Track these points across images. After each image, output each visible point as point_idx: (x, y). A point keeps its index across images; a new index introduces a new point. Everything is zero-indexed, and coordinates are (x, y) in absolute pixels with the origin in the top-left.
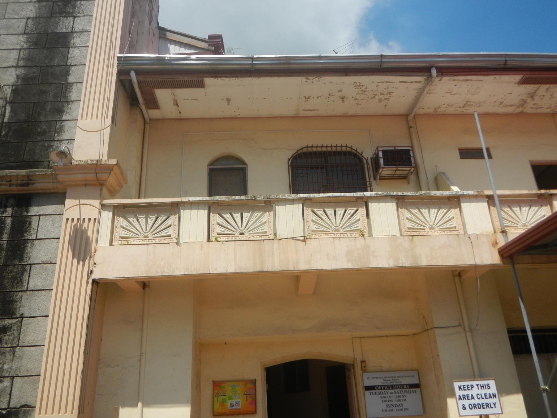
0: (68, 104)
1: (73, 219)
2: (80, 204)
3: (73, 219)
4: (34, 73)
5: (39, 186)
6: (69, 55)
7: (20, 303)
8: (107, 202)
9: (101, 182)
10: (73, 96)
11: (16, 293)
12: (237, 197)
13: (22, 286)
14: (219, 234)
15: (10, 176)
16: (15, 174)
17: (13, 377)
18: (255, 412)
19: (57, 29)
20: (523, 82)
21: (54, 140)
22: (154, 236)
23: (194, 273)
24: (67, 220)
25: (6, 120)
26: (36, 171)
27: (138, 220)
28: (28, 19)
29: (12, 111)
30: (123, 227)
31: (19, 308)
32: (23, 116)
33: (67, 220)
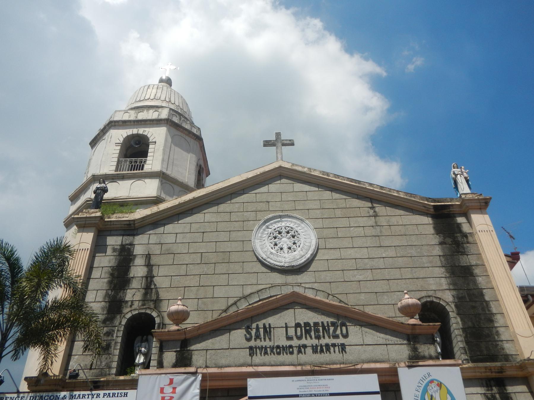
0: (494, 316)
4: (462, 294)
5: (509, 373)
6: (478, 282)
10: (494, 311)
15: (491, 367)
16: (494, 365)
19: (460, 263)
25: (461, 326)
28: (440, 256)
29: (462, 320)
32: (470, 324)
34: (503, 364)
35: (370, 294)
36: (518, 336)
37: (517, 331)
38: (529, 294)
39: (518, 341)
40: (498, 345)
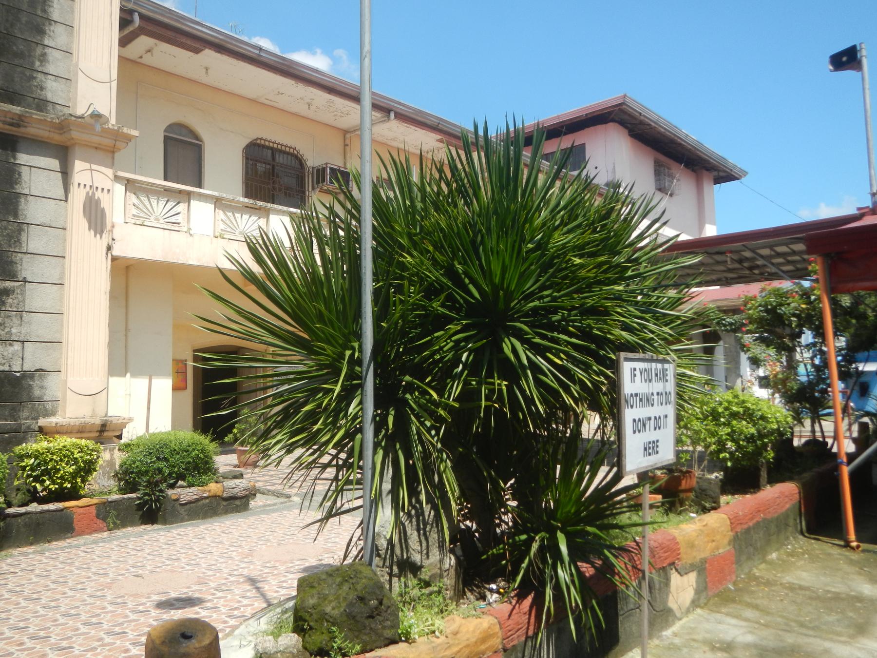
0: (50, 24)
1: (85, 185)
3: (85, 185)
5: (32, 131)
7: (21, 265)
8: (121, 174)
10: (55, 14)
11: (14, 254)
13: (21, 247)
17: (24, 341)
18: (186, 388)
20: (441, 141)
22: (166, 220)
23: (205, 265)
24: (79, 184)
26: (33, 114)
31: (21, 270)
33: (79, 184)
34: (27, 112)
36: (80, 72)
37: (81, 65)
38: (137, 12)
39: (77, 82)
40: (35, 78)
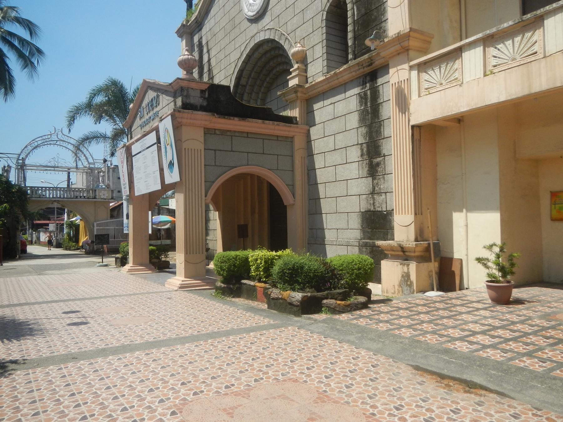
2: (398, 70)
3: (395, 83)
8: (412, 63)
9: (406, 48)
11: (379, 141)
12: (506, 25)
13: (381, 135)
14: (495, 66)
15: (361, 62)
21: (382, 22)
22: (447, 82)
23: (474, 107)
24: (392, 84)
26: (372, 53)
27: (434, 72)
30: (426, 81)
33: (392, 84)
35: (299, 14)
